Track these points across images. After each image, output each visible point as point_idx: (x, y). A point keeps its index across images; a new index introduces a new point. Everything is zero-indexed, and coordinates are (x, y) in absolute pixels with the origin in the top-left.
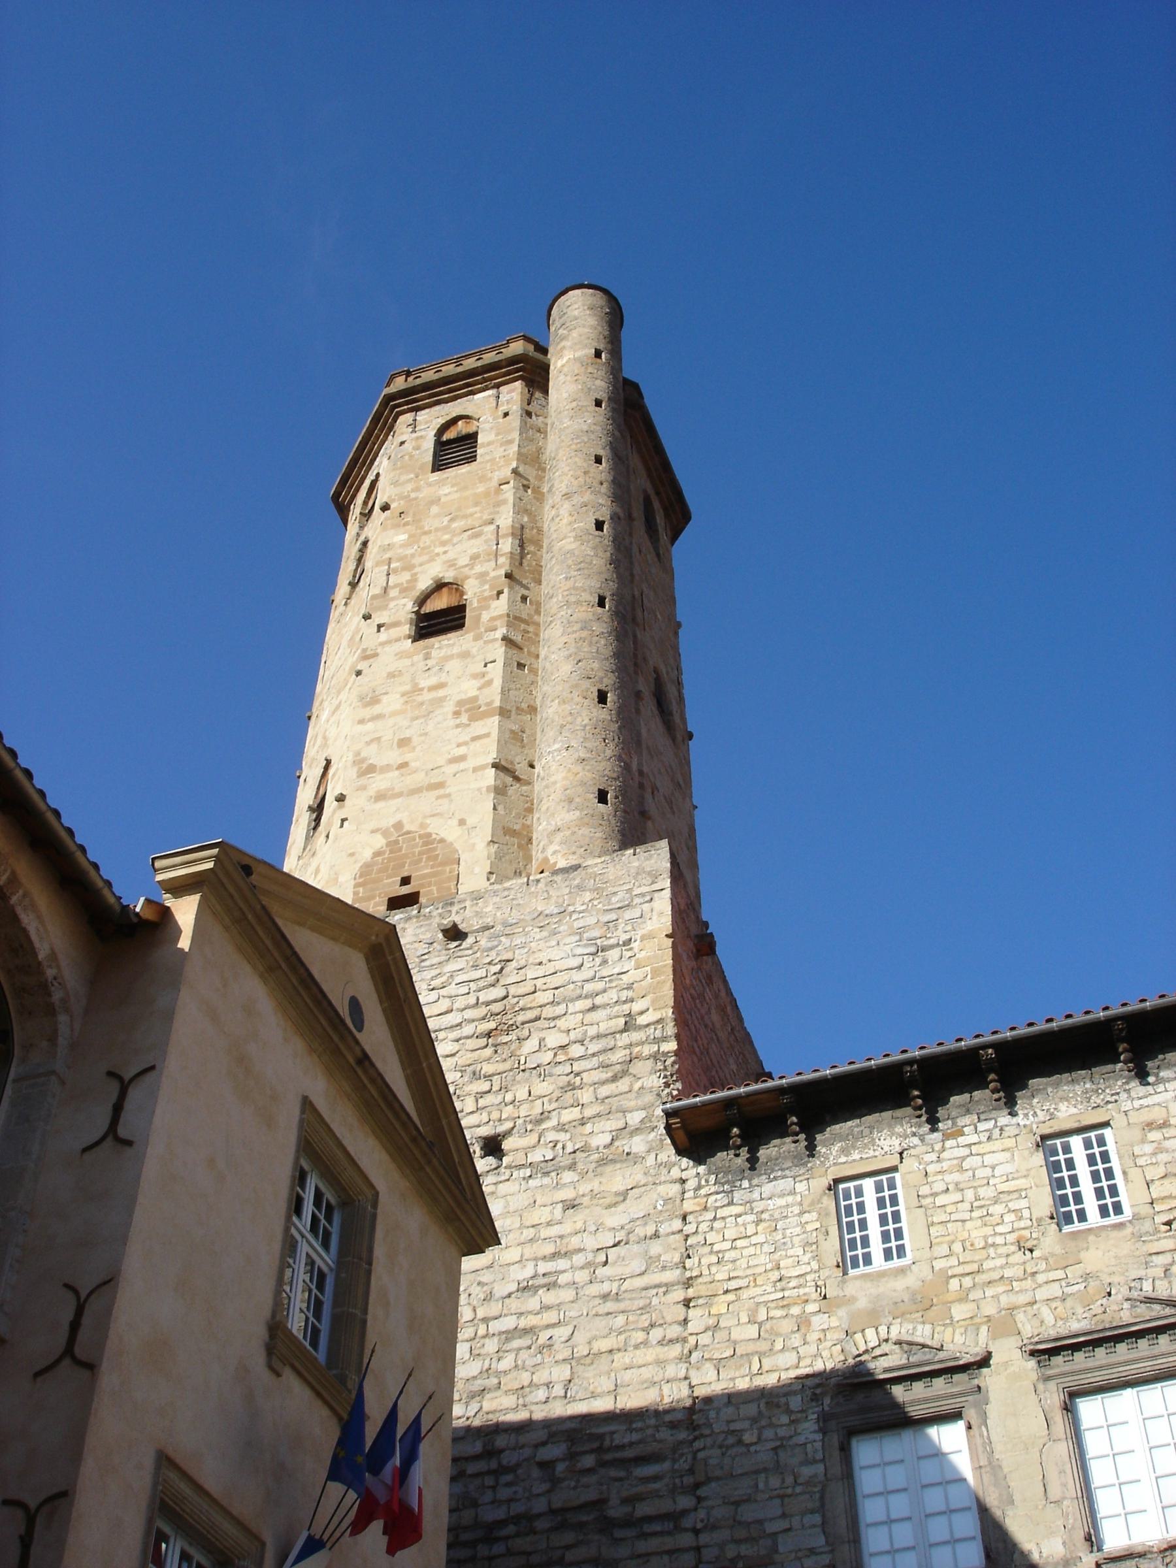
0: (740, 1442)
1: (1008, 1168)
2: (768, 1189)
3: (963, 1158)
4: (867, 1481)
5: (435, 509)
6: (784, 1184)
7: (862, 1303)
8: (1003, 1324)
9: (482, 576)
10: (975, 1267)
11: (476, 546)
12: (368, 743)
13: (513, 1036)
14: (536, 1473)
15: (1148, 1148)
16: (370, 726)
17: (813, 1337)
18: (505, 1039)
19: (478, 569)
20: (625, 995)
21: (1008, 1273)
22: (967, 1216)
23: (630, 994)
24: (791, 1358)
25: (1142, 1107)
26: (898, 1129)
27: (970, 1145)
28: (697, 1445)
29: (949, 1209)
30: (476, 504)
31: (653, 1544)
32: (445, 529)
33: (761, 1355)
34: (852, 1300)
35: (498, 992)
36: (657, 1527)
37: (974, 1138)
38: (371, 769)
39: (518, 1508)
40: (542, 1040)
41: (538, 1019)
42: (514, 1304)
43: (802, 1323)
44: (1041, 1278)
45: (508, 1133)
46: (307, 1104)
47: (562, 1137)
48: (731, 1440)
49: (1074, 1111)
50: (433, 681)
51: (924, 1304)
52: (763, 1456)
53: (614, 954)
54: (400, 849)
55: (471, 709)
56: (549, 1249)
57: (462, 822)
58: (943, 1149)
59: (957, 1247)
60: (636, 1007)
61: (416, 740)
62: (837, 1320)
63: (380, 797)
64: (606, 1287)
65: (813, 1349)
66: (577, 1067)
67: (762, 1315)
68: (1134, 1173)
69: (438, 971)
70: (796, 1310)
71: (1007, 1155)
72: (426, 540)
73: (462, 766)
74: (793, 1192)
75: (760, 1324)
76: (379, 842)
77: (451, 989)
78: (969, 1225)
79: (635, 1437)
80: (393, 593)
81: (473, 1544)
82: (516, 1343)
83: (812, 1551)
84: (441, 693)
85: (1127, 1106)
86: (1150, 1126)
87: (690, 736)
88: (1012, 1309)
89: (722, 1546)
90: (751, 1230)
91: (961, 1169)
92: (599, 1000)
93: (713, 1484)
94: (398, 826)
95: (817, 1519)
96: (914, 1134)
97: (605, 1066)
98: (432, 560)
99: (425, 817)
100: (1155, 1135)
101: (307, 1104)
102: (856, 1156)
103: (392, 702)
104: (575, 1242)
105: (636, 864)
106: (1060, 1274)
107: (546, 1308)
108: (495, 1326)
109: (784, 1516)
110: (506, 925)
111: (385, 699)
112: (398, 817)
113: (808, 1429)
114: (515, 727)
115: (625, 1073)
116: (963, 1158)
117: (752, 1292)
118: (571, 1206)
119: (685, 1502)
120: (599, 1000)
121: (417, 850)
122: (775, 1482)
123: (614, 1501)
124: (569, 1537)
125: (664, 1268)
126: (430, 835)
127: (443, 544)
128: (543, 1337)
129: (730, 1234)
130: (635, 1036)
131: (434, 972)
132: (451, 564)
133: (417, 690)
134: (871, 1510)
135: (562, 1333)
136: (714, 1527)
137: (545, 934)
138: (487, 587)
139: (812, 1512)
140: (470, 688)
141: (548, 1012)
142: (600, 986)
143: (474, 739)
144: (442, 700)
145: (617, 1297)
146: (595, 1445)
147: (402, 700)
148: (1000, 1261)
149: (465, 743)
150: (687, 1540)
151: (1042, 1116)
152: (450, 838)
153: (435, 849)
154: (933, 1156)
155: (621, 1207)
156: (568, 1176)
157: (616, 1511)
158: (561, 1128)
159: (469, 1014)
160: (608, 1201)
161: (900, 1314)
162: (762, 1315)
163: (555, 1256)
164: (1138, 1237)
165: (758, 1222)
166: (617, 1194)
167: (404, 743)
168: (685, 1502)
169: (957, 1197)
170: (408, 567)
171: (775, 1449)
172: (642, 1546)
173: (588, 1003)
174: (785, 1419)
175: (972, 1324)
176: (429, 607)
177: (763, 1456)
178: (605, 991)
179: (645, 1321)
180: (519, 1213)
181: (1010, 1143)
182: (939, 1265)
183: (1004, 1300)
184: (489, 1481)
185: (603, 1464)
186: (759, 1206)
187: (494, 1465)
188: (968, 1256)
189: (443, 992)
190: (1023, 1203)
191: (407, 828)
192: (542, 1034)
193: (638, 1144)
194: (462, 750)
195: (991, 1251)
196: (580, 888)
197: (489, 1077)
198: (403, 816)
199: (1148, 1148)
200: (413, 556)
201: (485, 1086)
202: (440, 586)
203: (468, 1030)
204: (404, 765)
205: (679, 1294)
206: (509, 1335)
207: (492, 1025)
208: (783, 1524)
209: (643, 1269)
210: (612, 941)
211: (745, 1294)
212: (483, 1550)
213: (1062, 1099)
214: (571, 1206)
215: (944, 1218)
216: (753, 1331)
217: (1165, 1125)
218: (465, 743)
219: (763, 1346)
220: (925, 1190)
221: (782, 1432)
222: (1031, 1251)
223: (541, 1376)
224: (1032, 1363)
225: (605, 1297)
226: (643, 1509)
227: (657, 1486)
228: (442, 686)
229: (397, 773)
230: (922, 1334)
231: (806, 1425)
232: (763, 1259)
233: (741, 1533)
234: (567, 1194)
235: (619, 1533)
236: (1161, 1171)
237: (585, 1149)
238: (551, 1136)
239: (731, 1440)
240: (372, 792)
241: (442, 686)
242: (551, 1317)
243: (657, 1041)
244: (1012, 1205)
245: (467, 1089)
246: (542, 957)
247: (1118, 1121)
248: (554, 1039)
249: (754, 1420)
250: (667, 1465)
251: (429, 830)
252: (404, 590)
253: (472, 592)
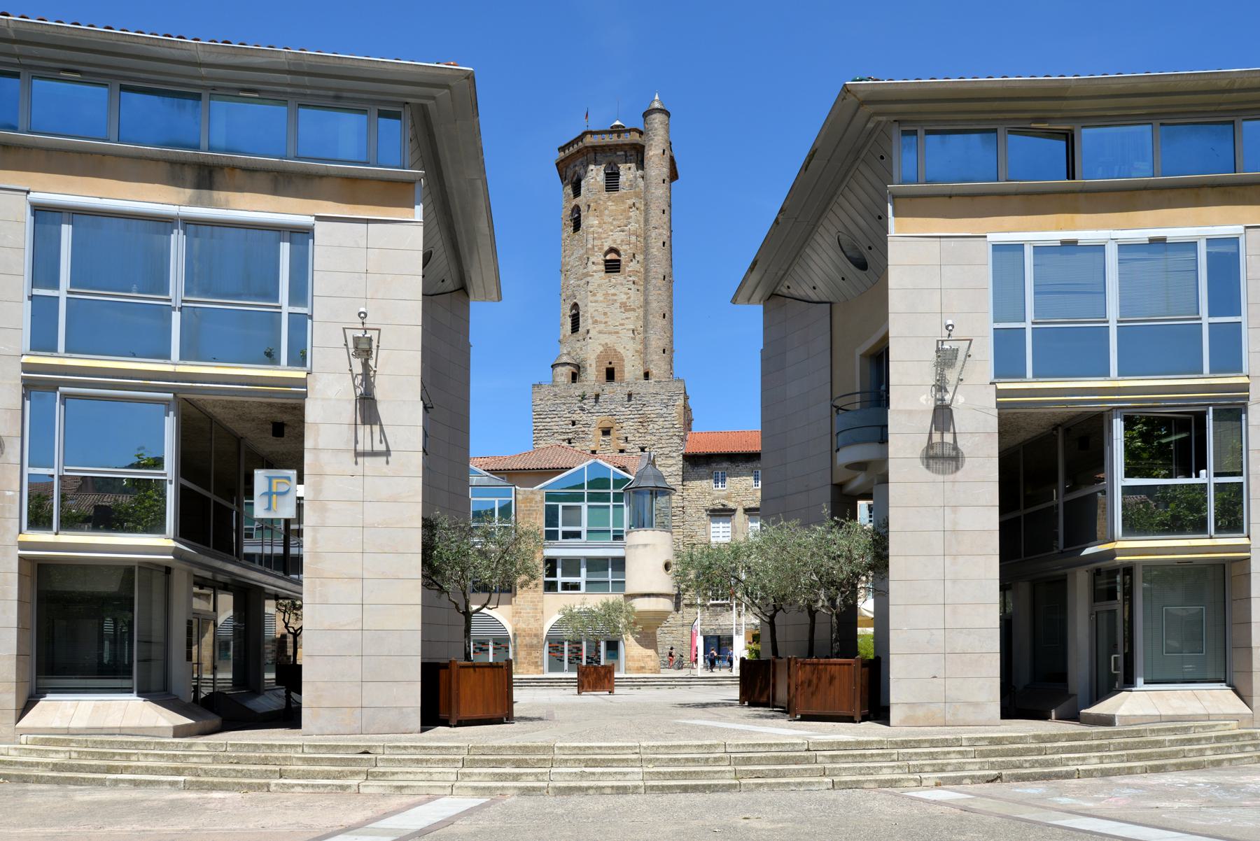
8: (740, 503)
38: (595, 322)
51: (728, 497)
55: (625, 307)
76: (601, 349)
132: (615, 241)
133: (607, 294)
140: (623, 298)
167: (605, 314)
170: (600, 238)
176: (608, 257)
202: (612, 250)
230: (726, 502)
253: (623, 258)
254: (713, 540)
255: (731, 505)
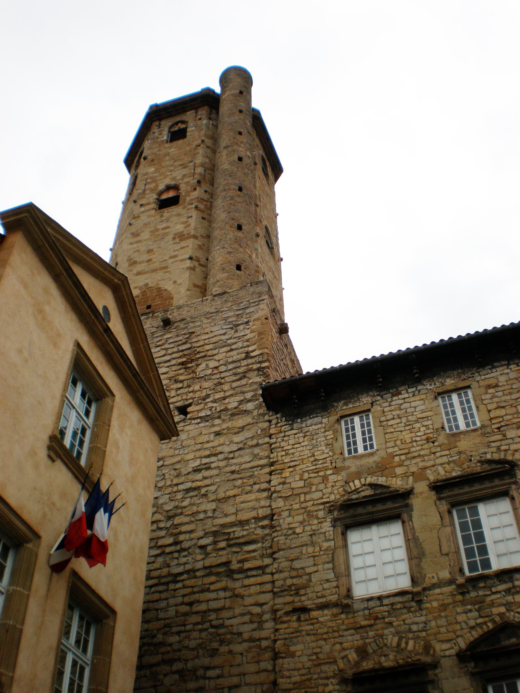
0: (294, 533)
1: (423, 407)
2: (309, 422)
3: (401, 404)
4: (354, 549)
5: (167, 158)
6: (316, 420)
7: (353, 469)
8: (419, 476)
9: (187, 183)
10: (406, 451)
11: (185, 171)
12: (134, 252)
13: (193, 364)
14: (198, 551)
15: (488, 396)
16: (135, 245)
17: (330, 485)
18: (190, 365)
19: (186, 180)
20: (246, 344)
21: (422, 453)
22: (403, 429)
23: (248, 343)
24: (320, 494)
25: (485, 379)
26: (371, 393)
27: (404, 399)
28: (274, 535)
29: (394, 426)
30: (185, 155)
31: (252, 580)
32: (171, 166)
33: (305, 494)
34: (349, 467)
35: (188, 346)
36: (254, 573)
37: (407, 395)
38: (135, 262)
39: (188, 567)
40: (207, 365)
41: (205, 356)
42: (190, 477)
43: (325, 479)
44: (438, 454)
45: (190, 405)
46: (78, 345)
47: (214, 405)
48: (290, 532)
49: (453, 382)
50: (164, 225)
51: (384, 467)
52: (305, 538)
53: (241, 327)
54: (147, 294)
55: (181, 237)
56: (208, 453)
57: (175, 282)
58: (392, 401)
59: (398, 442)
60: (251, 349)
61: (155, 250)
62: (341, 477)
63: (138, 274)
64: (233, 468)
65: (329, 490)
66: (223, 375)
67: (306, 476)
68: (481, 407)
69: (160, 339)
70: (321, 474)
71: (422, 402)
72: (163, 170)
73: (176, 259)
74: (321, 423)
75: (305, 480)
77: (166, 346)
78: (403, 433)
79: (245, 533)
80: (147, 192)
81: (167, 583)
82: (192, 494)
83: (328, 581)
84: (167, 230)
85: (478, 378)
86: (489, 387)
87: (282, 260)
88: (426, 468)
89: (285, 579)
90: (301, 440)
91: (400, 409)
92: (233, 347)
93: (281, 552)
94: (147, 284)
95: (330, 565)
96: (378, 395)
97: (235, 374)
98: (165, 178)
99: (159, 281)
100: (490, 391)
101: (78, 345)
102: (351, 406)
103: (145, 235)
104: (220, 449)
105: (252, 290)
106: (447, 452)
107: (205, 478)
108: (181, 487)
109: (315, 565)
110: (191, 318)
111: (142, 234)
112: (146, 281)
113: (327, 526)
114: (199, 243)
115: (245, 377)
116: (401, 404)
117: (301, 467)
118: (218, 434)
119: (267, 561)
120: (233, 347)
121: (154, 295)
122: (310, 549)
123: (234, 562)
124: (213, 579)
125: (260, 459)
126: (160, 288)
127: (171, 171)
128: (203, 491)
129: (291, 442)
130: (250, 361)
131: (158, 339)
132: (174, 179)
134: (355, 563)
135: (213, 488)
136: (281, 572)
137: (209, 321)
138: (189, 187)
139: (328, 563)
140: (180, 228)
141: (210, 353)
142: (235, 341)
143: (181, 248)
144: (167, 234)
145: (238, 472)
146: (227, 537)
147: (150, 234)
148: (418, 448)
149: (177, 250)
150: (268, 578)
151: (438, 384)
152: (169, 289)
153: (162, 294)
154: (387, 404)
155: (241, 434)
156: (217, 422)
157: (235, 566)
158: (214, 401)
159: (174, 356)
160: (236, 430)
161: (371, 472)
162: (306, 476)
163: (209, 456)
164: (484, 435)
165: (304, 437)
166: (239, 428)
167: (150, 251)
168: (267, 561)
169: (399, 421)
170: (155, 181)
171: (311, 535)
172: (247, 582)
173: (228, 348)
174: (316, 522)
175: (405, 476)
177: (305, 538)
178: (236, 343)
179: (251, 481)
180: (194, 438)
181: (423, 397)
182: (390, 450)
183: (421, 465)
184: (176, 555)
185: (230, 546)
186: (306, 429)
187: (178, 547)
188: (403, 446)
189: (163, 347)
190: (429, 422)
191: (150, 285)
192: (207, 363)
193: (250, 406)
194: (176, 253)
195: (414, 444)
196: (226, 301)
197: (182, 381)
198: (149, 281)
199: (488, 396)
200: (157, 177)
201: (180, 385)
202: (168, 188)
203: (173, 362)
204: (150, 260)
205: (267, 470)
206: (188, 490)
207: (184, 359)
208: (315, 568)
209: (251, 459)
210: (240, 322)
211: (298, 468)
212: (172, 586)
213: (448, 377)
214: (218, 434)
215: (393, 430)
216: (301, 483)
217: (497, 386)
218: (177, 250)
219: (306, 490)
220: (383, 419)
221: (314, 527)
222: (433, 443)
223: (203, 508)
224: (433, 493)
225: (233, 472)
226: (247, 565)
227: (255, 554)
228: (168, 227)
229: (146, 264)
230: (382, 480)
231: (325, 524)
232: (307, 452)
233: (294, 573)
234: (217, 429)
235: (236, 576)
236: (495, 405)
237: (226, 410)
238: (210, 405)
239: (290, 532)
240: (135, 271)
241: (168, 227)
242: (208, 482)
243: (260, 362)
244: (425, 423)
245: (172, 387)
246: (207, 330)
247: (474, 385)
248: (212, 364)
249: (301, 523)
250: (260, 545)
251: (160, 286)
252: (152, 190)
254: (359, 591)
255: (397, 484)
